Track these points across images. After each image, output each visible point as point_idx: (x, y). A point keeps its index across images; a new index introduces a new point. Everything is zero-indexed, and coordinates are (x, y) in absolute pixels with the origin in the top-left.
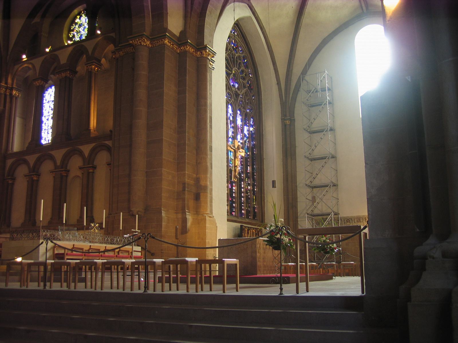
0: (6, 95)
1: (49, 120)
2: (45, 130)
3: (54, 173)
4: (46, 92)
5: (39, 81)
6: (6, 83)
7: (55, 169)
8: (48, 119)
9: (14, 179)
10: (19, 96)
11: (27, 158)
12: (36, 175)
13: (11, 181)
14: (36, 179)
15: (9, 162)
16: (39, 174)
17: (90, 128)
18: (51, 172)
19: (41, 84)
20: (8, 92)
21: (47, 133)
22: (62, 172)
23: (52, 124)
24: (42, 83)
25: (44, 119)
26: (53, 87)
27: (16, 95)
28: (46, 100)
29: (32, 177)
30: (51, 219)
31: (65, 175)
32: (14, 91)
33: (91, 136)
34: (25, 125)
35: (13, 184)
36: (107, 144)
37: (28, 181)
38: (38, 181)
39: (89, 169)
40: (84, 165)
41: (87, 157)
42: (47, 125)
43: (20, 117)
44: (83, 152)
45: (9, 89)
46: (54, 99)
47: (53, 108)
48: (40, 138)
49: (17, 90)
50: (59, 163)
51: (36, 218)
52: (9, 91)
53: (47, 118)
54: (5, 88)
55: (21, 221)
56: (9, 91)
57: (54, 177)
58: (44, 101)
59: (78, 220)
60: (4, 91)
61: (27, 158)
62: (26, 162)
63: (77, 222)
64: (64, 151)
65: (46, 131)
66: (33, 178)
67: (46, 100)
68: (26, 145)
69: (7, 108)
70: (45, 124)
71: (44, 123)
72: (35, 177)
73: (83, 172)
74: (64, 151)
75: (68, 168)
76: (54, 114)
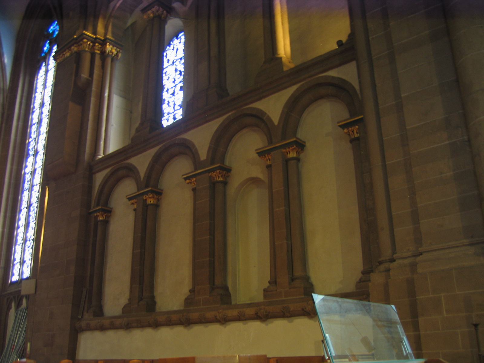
0: (93, 55)
1: (175, 94)
2: (168, 114)
3: (194, 179)
4: (168, 47)
5: (154, 9)
6: (95, 33)
7: (196, 169)
8: (173, 94)
9: (108, 212)
10: (118, 56)
11: (133, 161)
12: (152, 192)
13: (102, 215)
14: (152, 202)
15: (99, 178)
16: (160, 191)
17: (279, 55)
18: (186, 179)
19: (157, 14)
20: (97, 48)
21: (175, 101)
22: (213, 174)
23: (182, 99)
24: (160, 12)
25: (166, 96)
26: (182, 36)
27: (112, 53)
28: (168, 61)
29: (145, 198)
30: (192, 291)
31: (221, 179)
32: (108, 46)
33: (285, 69)
34: (131, 112)
35: (106, 223)
36: (333, 78)
37: (135, 210)
38: (157, 206)
39: (288, 150)
40: (270, 142)
41: (276, 123)
42: (171, 104)
43: (121, 96)
44: (266, 114)
45: (100, 44)
46: (184, 55)
47: (182, 70)
48: (160, 114)
49: (114, 44)
50: (203, 155)
51: (154, 293)
52: (101, 48)
53: (171, 91)
54: (92, 42)
55: (124, 301)
56: (100, 46)
57: (194, 190)
58: (165, 64)
59: (265, 290)
60: (90, 47)
61: (133, 161)
62: (131, 171)
63: (265, 297)
64: (214, 125)
65: (172, 116)
66: (146, 200)
67: (168, 61)
68: (133, 132)
69: (95, 76)
70: (169, 102)
71: (166, 102)
72: (150, 198)
73: (269, 163)
74: (214, 125)
75: (227, 163)
76: (185, 81)
